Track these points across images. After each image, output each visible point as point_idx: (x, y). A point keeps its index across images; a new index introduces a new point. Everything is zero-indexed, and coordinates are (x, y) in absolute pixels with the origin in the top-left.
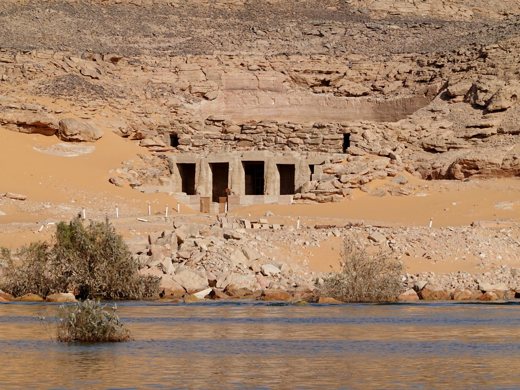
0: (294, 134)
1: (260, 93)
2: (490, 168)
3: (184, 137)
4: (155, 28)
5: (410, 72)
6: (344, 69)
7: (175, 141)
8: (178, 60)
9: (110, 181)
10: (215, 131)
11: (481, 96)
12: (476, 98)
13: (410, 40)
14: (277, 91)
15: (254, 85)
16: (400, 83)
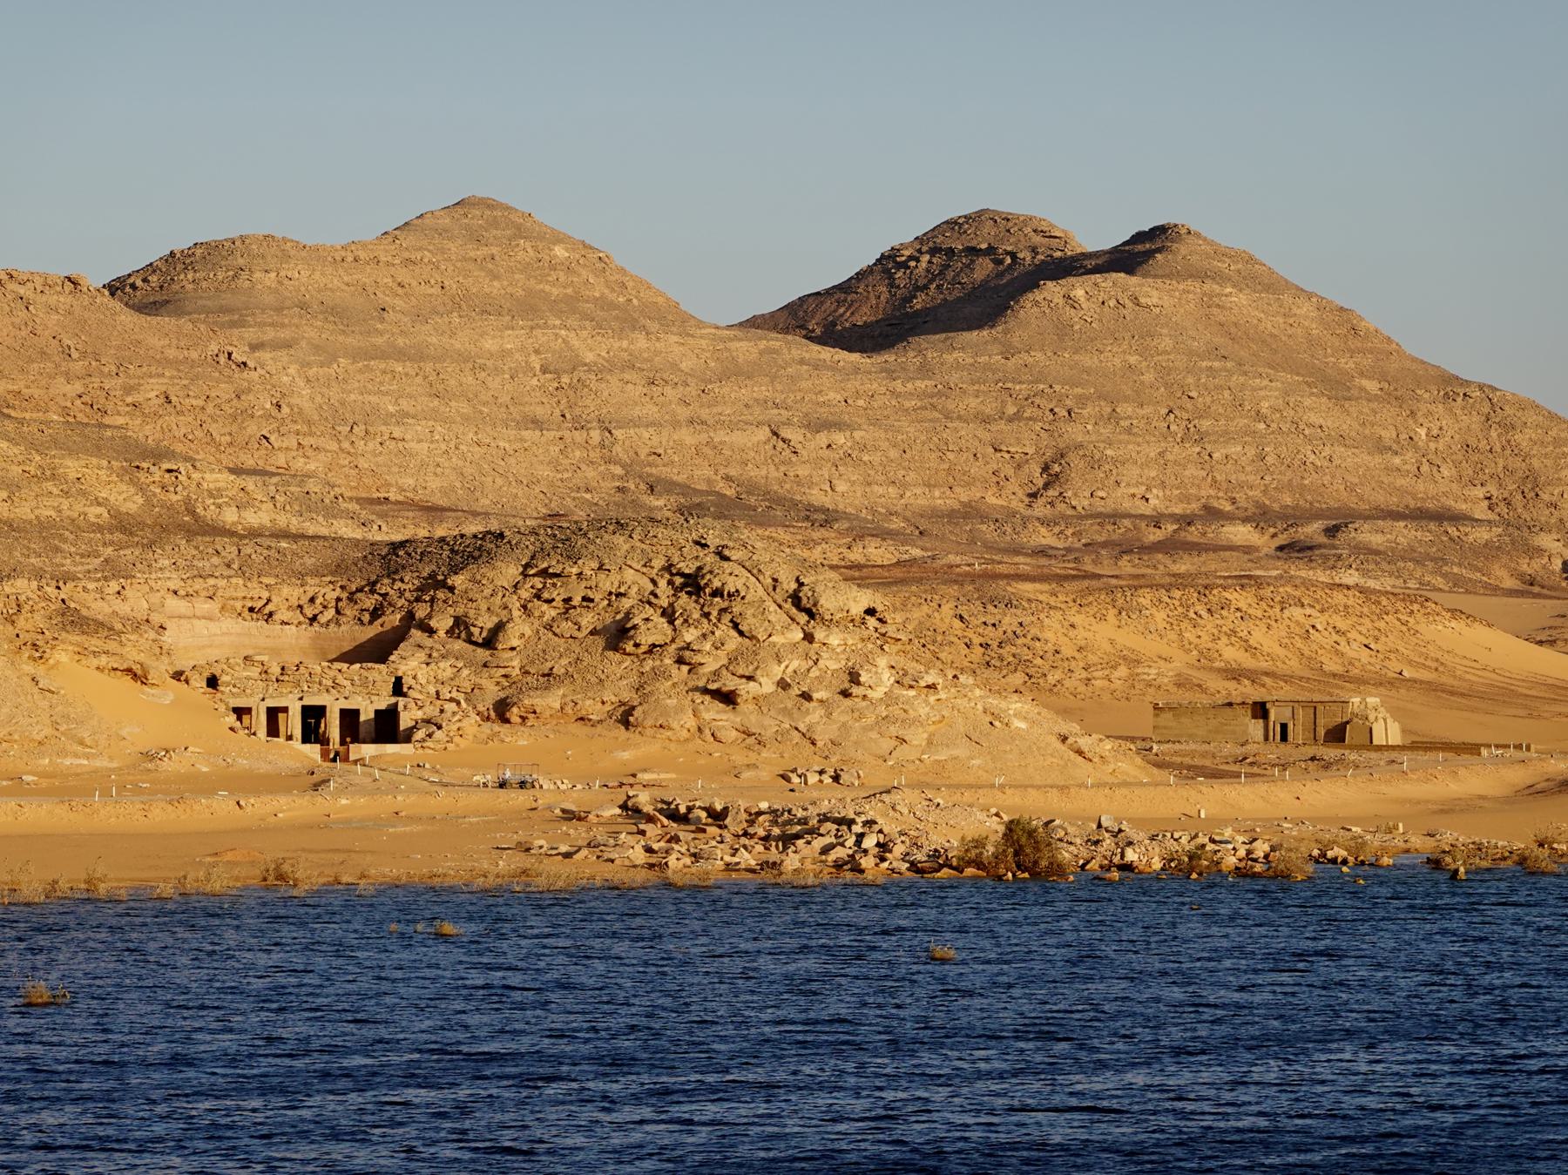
0: (340, 677)
1: (196, 622)
2: (548, 713)
3: (225, 678)
4: (65, 547)
5: (338, 599)
6: (265, 595)
7: (213, 682)
8: (114, 586)
9: (231, 729)
10: (254, 672)
11: (476, 631)
12: (470, 634)
13: (309, 561)
14: (210, 619)
15: (189, 613)
16: (332, 612)
